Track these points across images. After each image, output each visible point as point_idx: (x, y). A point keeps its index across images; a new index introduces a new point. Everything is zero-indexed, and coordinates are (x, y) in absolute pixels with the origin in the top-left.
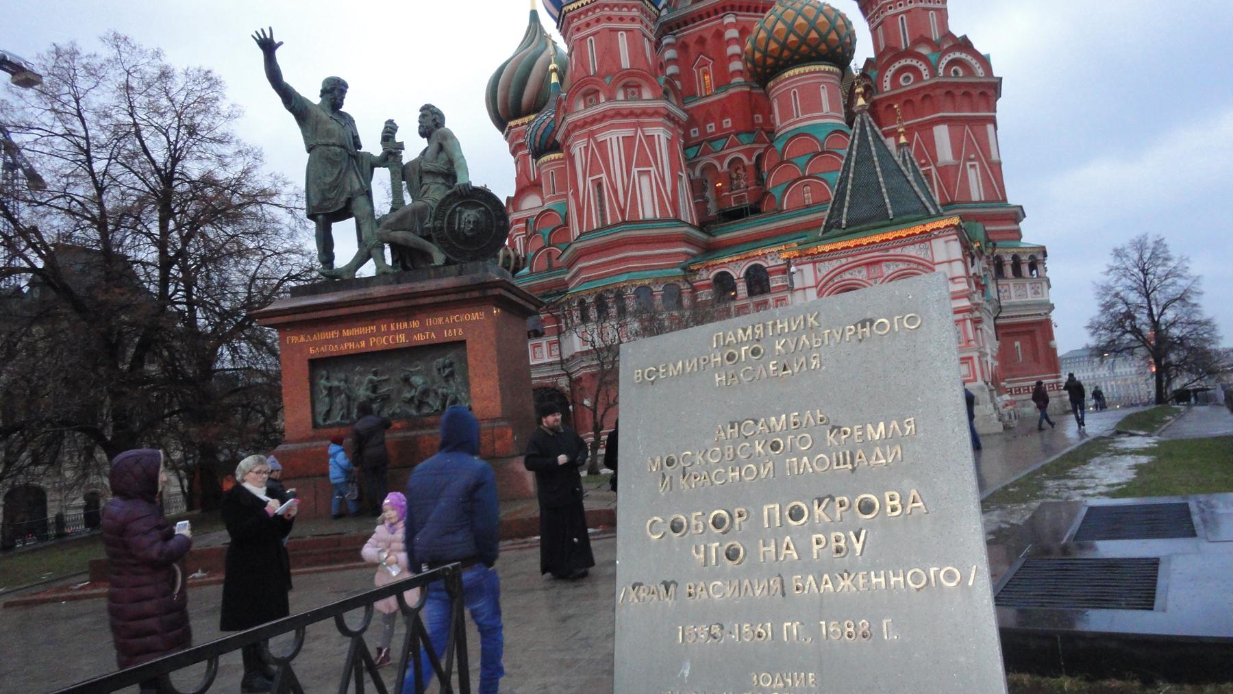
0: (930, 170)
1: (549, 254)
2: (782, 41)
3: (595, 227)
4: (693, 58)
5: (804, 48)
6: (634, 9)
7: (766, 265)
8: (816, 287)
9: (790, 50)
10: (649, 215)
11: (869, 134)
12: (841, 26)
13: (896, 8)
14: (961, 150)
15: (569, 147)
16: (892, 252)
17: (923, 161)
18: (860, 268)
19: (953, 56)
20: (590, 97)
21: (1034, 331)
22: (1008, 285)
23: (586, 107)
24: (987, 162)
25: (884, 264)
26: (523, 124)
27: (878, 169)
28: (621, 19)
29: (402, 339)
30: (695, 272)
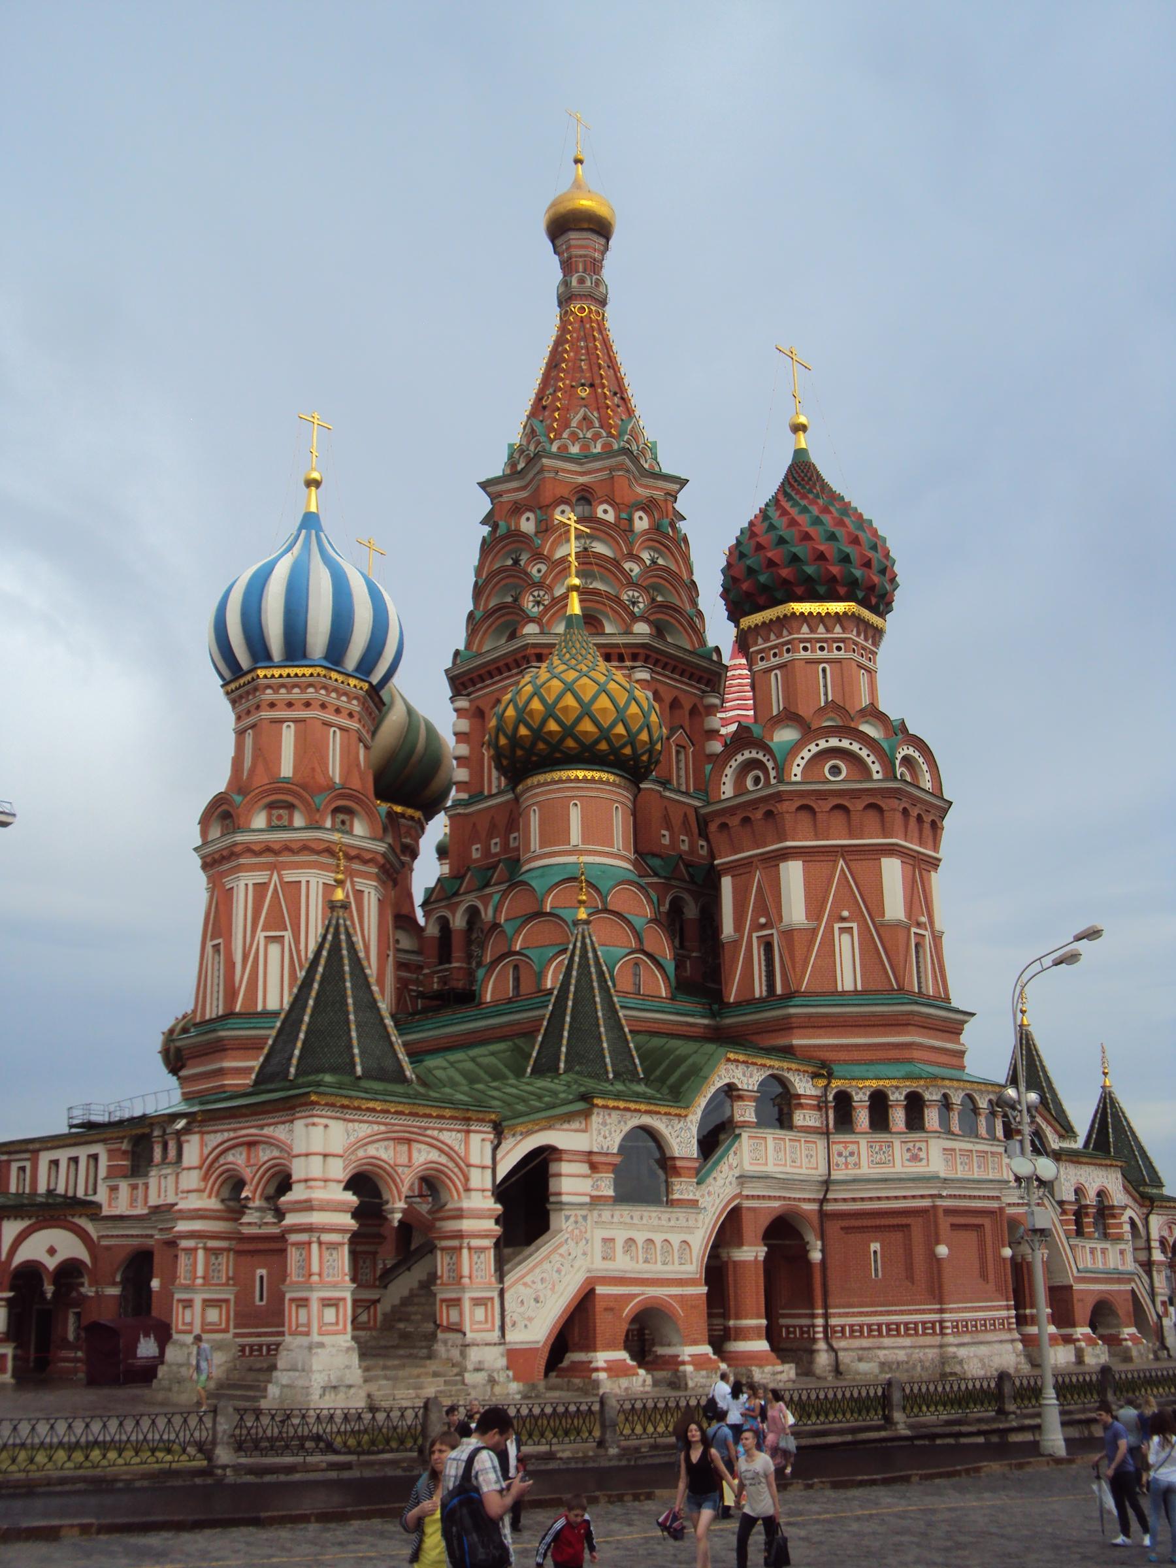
5: (541, 746)
6: (311, 690)
8: (200, 1168)
12: (604, 710)
13: (769, 659)
14: (825, 901)
16: (266, 1131)
17: (763, 920)
19: (823, 745)
21: (908, 1226)
22: (858, 1143)
23: (223, 835)
25: (261, 1147)
28: (290, 705)
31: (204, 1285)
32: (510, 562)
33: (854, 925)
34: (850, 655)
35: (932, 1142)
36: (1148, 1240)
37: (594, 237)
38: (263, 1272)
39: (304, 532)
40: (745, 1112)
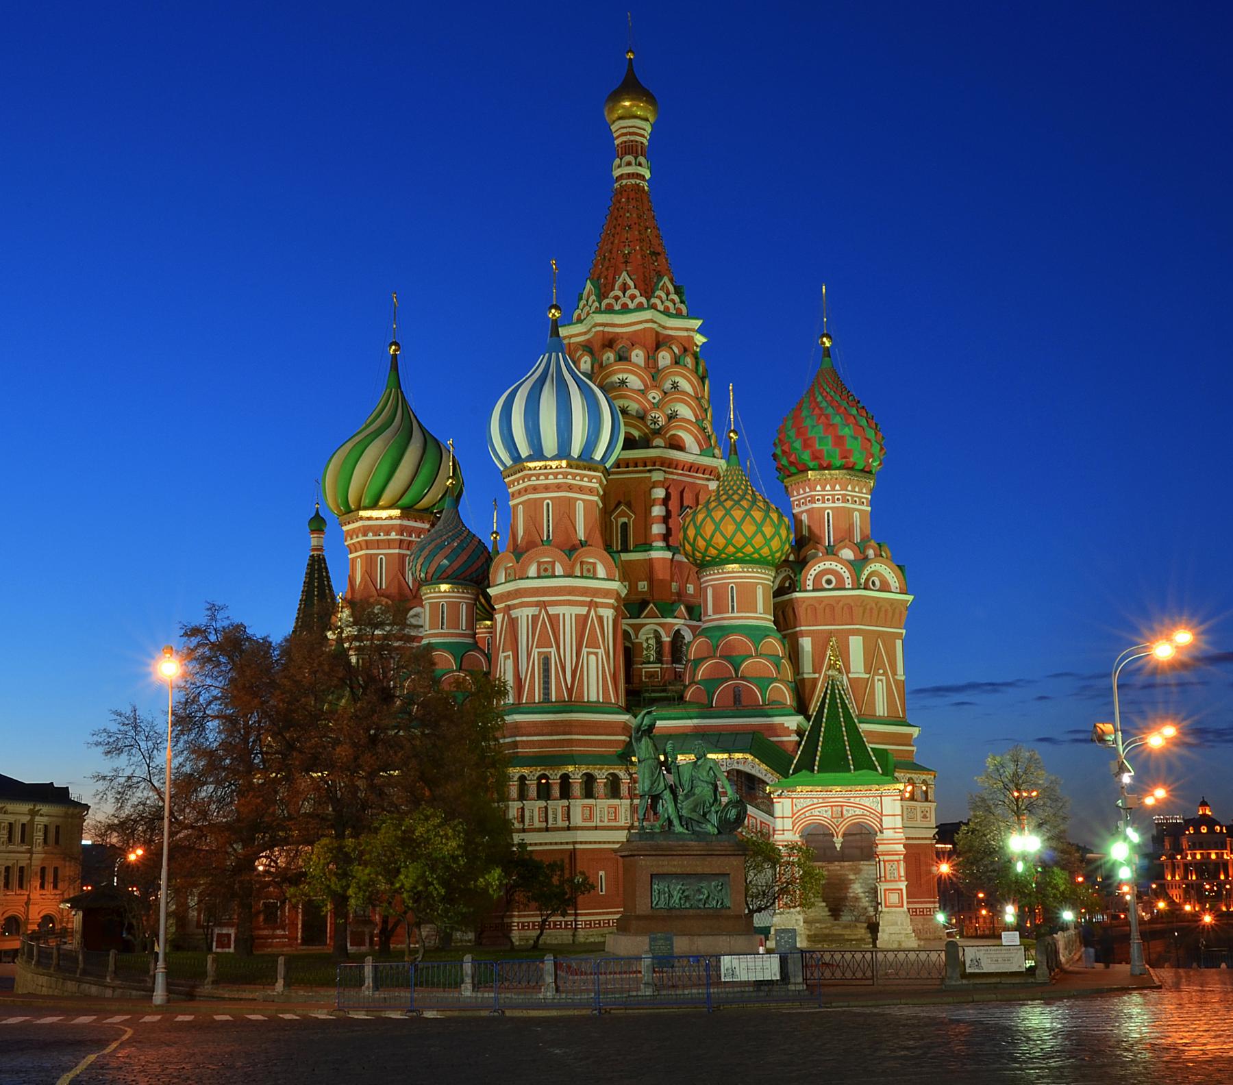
3: (537, 701)
4: (612, 507)
6: (594, 480)
9: (734, 547)
10: (593, 698)
11: (838, 696)
13: (824, 502)
15: (509, 608)
16: (852, 800)
20: (546, 566)
24: (893, 678)
25: (845, 808)
26: (377, 519)
27: (844, 729)
28: (581, 489)
29: (700, 870)
33: (884, 678)
38: (602, 873)
39: (560, 354)
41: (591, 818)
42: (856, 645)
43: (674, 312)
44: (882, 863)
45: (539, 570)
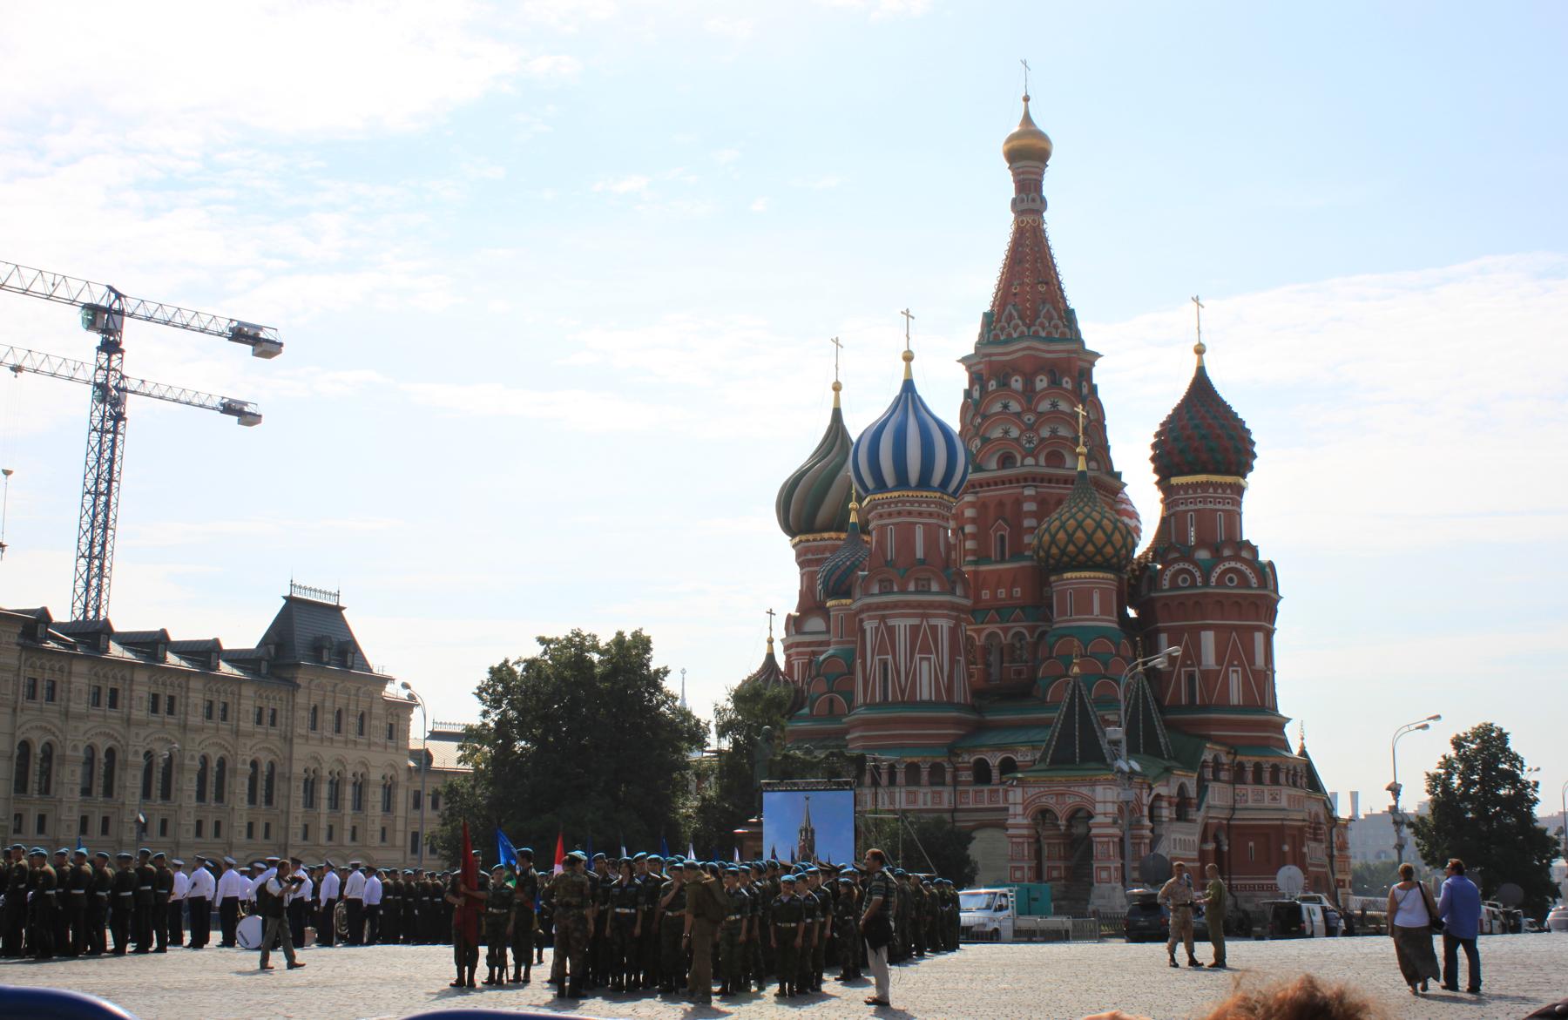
0: (1194, 671)
1: (831, 701)
2: (1062, 547)
3: (878, 700)
6: (933, 506)
7: (1015, 758)
8: (1023, 804)
10: (925, 696)
11: (1077, 696)
13: (1187, 505)
15: (861, 621)
16: (1072, 789)
17: (1189, 662)
18: (1051, 796)
19: (1227, 565)
20: (885, 584)
25: (1067, 796)
26: (814, 540)
28: (920, 514)
30: (958, 755)
31: (1029, 859)
32: (997, 408)
33: (1240, 669)
34: (1234, 508)
35: (1283, 791)
36: (1332, 842)
37: (1040, 165)
39: (910, 394)
40: (1209, 774)
41: (915, 802)
42: (1208, 639)
43: (1057, 336)
44: (1094, 844)
45: (880, 590)
